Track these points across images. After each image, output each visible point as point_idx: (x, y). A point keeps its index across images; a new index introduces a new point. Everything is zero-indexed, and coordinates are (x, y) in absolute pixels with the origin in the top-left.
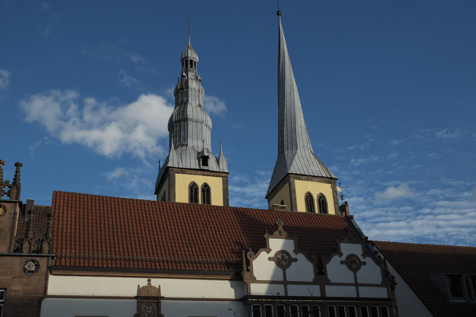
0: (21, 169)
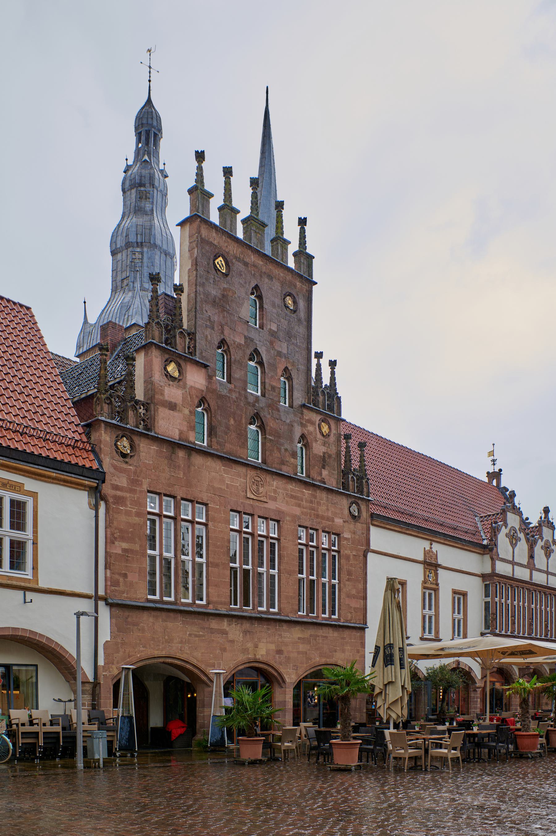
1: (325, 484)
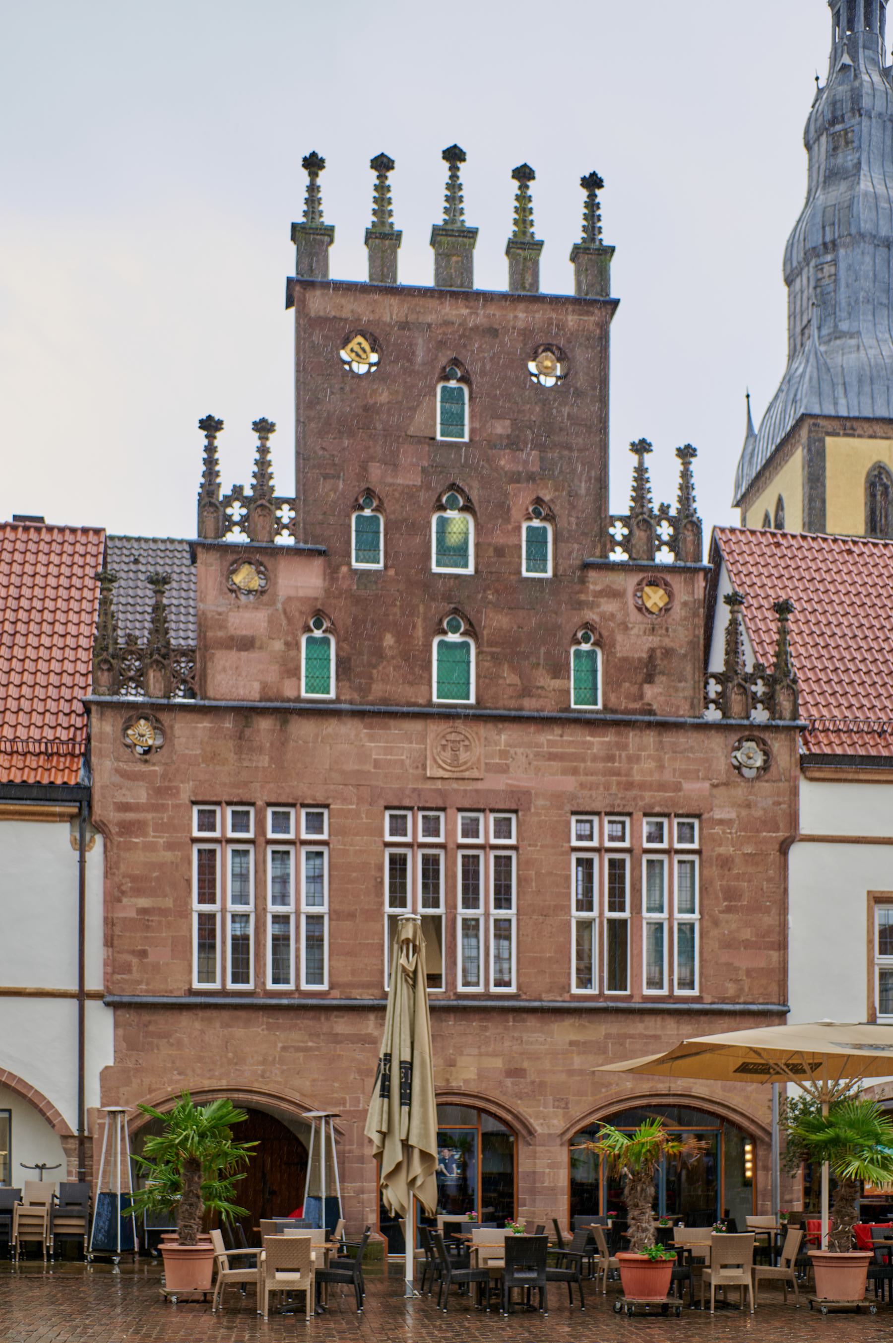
0: (695, 465)
1: (655, 714)
